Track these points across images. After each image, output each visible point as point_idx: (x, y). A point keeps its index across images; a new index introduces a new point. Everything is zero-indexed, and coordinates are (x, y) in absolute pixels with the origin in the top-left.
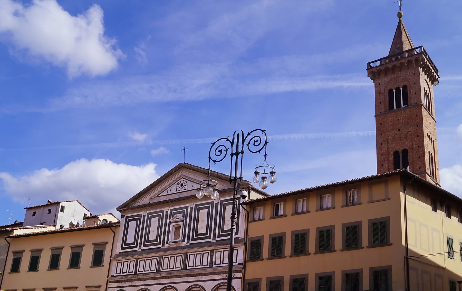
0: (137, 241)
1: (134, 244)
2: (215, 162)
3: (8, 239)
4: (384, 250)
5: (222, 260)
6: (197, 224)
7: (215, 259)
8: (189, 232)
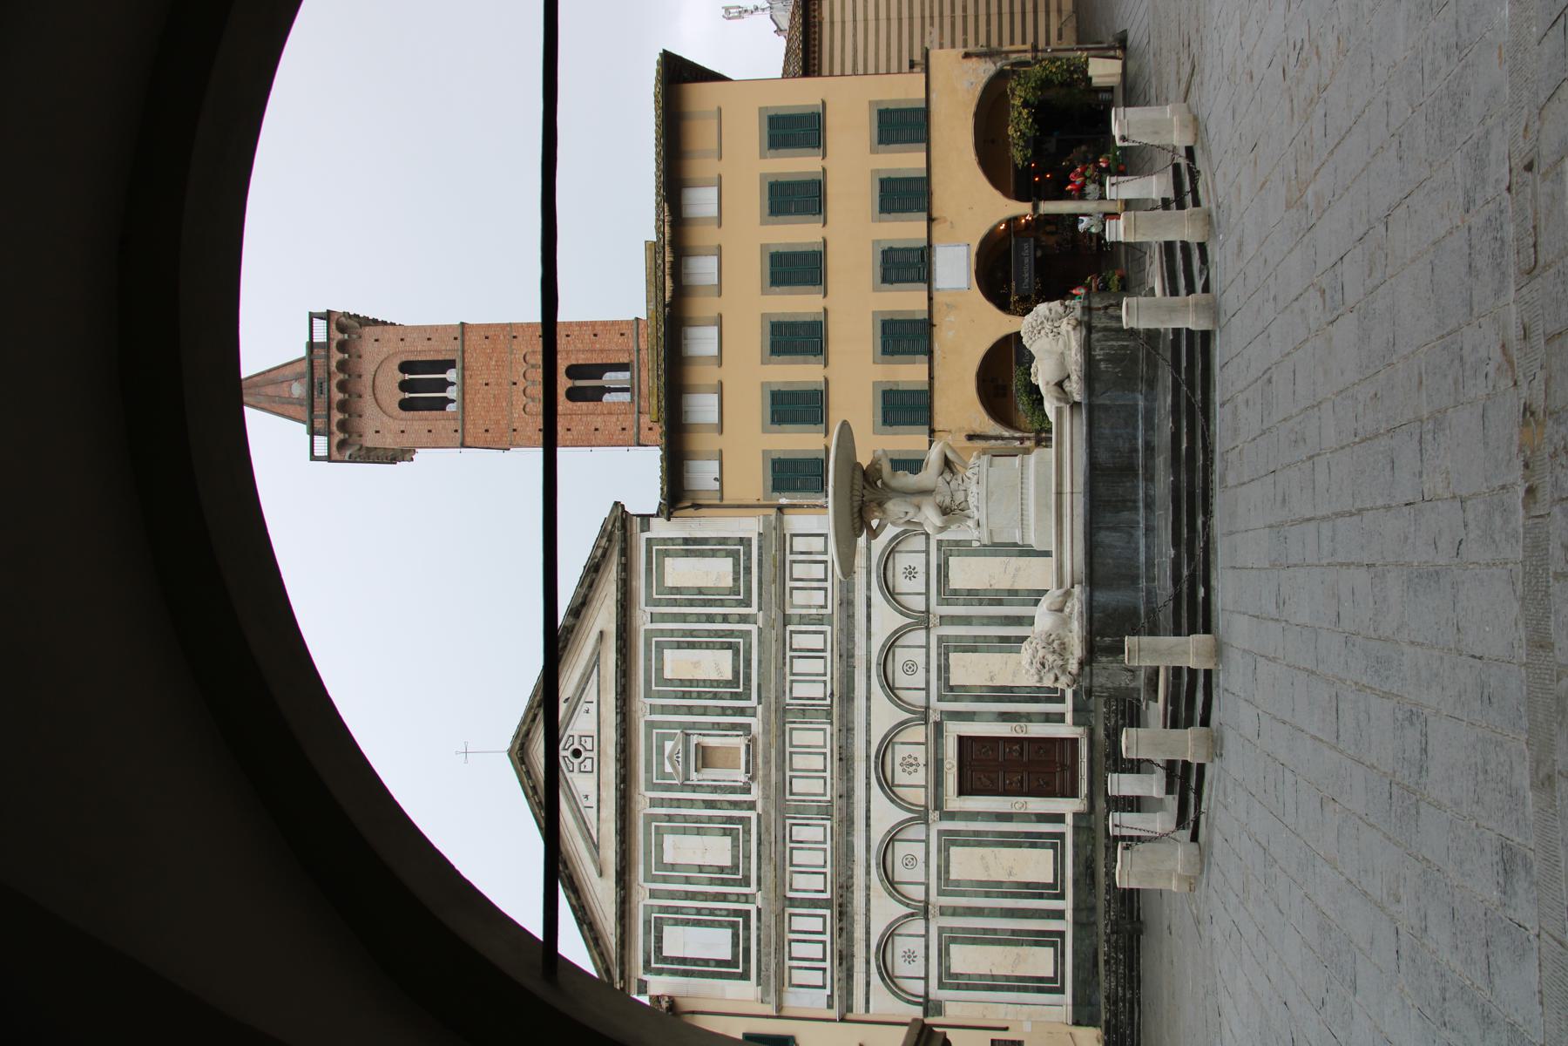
1: (737, 923)
4: (832, 122)
6: (705, 682)
7: (810, 607)
8: (724, 711)
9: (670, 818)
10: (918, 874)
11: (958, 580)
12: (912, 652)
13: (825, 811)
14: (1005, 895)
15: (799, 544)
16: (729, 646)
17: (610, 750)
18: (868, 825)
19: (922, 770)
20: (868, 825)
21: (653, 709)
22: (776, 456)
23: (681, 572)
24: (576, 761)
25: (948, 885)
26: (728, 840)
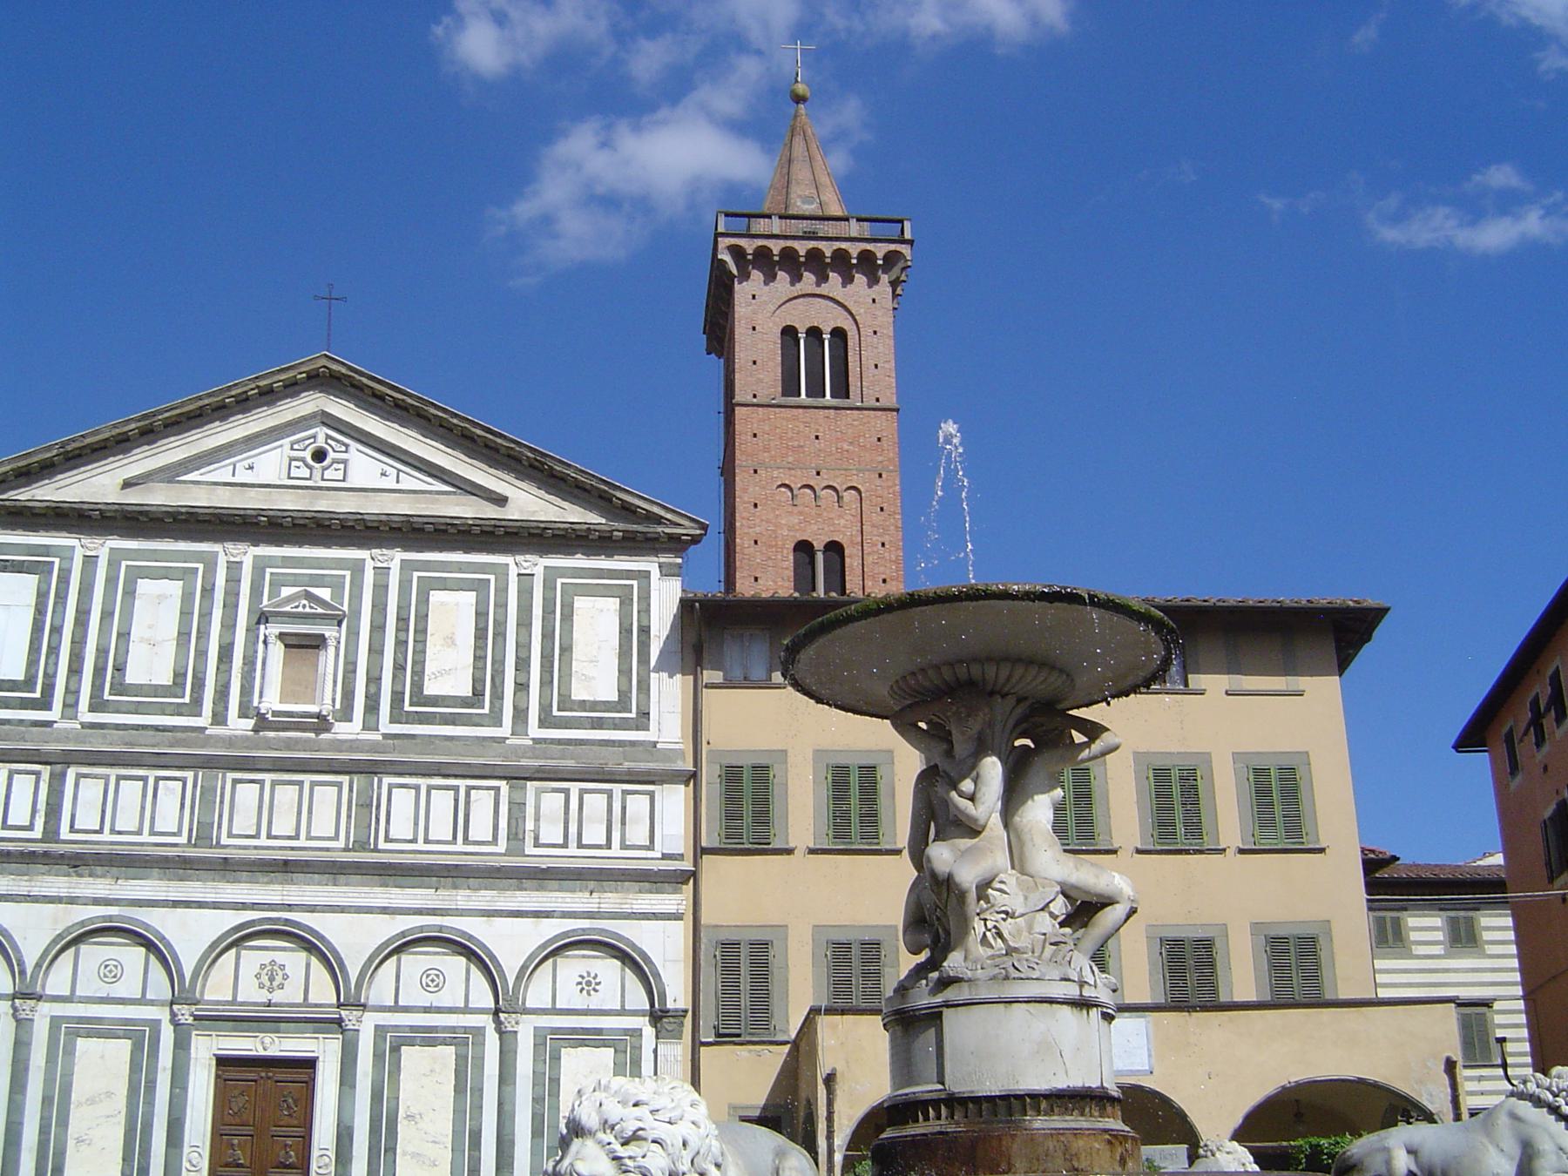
5: (573, 829)
6: (421, 652)
7: (537, 819)
8: (374, 679)
9: (208, 591)
10: (89, 985)
12: (457, 981)
13: (203, 835)
14: (44, 1130)
16: (478, 693)
17: (323, 504)
18: (176, 904)
19: (263, 996)
20: (176, 904)
21: (382, 572)
22: (776, 770)
23: (596, 623)
24: (308, 455)
25: (68, 1033)
26: (167, 679)
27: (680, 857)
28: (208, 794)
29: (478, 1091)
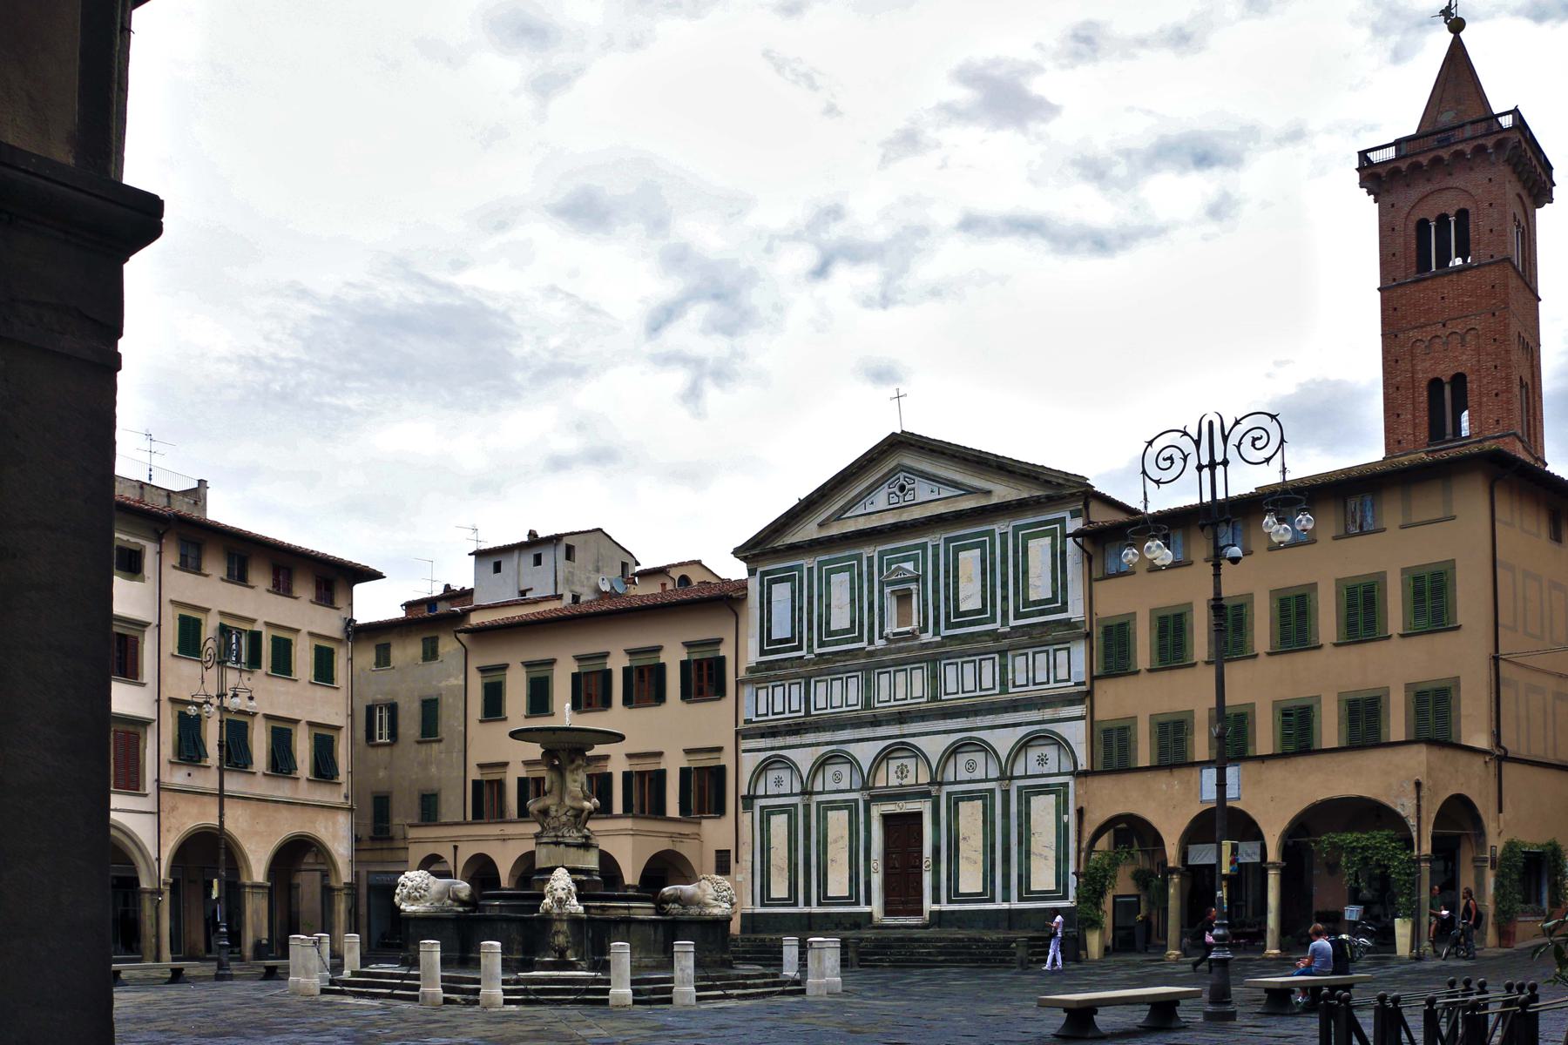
0: (801, 633)
2: (1158, 482)
3: (461, 636)
4: (1440, 640)
6: (956, 588)
8: (936, 608)
9: (860, 575)
11: (1036, 802)
15: (1062, 656)
17: (906, 516)
21: (936, 547)
23: (1039, 552)
24: (896, 490)
26: (847, 625)
27: (1083, 683)
28: (868, 681)
29: (993, 823)
